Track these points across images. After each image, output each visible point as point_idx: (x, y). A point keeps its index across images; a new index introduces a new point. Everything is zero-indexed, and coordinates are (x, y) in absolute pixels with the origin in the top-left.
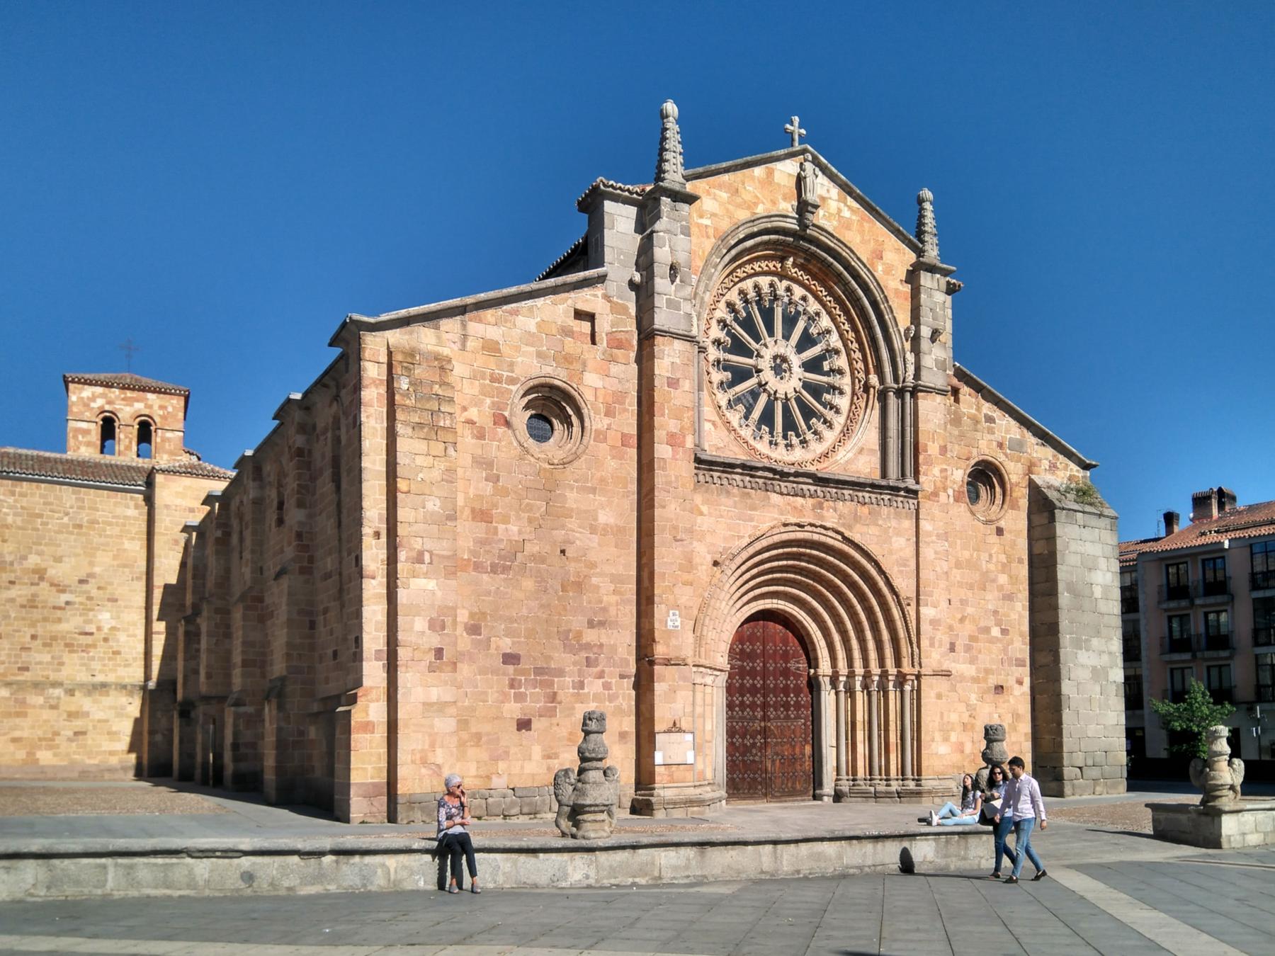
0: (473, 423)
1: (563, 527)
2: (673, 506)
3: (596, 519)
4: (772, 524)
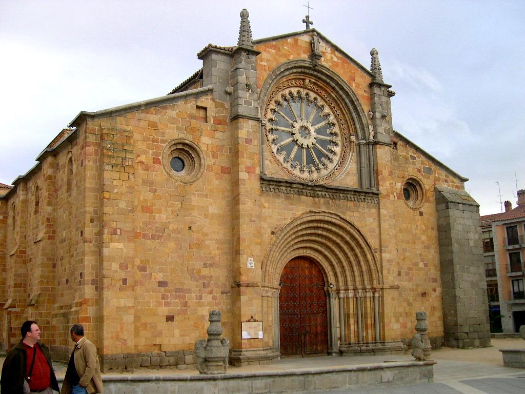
1: (190, 215)
2: (249, 203)
3: (207, 211)
4: (302, 212)
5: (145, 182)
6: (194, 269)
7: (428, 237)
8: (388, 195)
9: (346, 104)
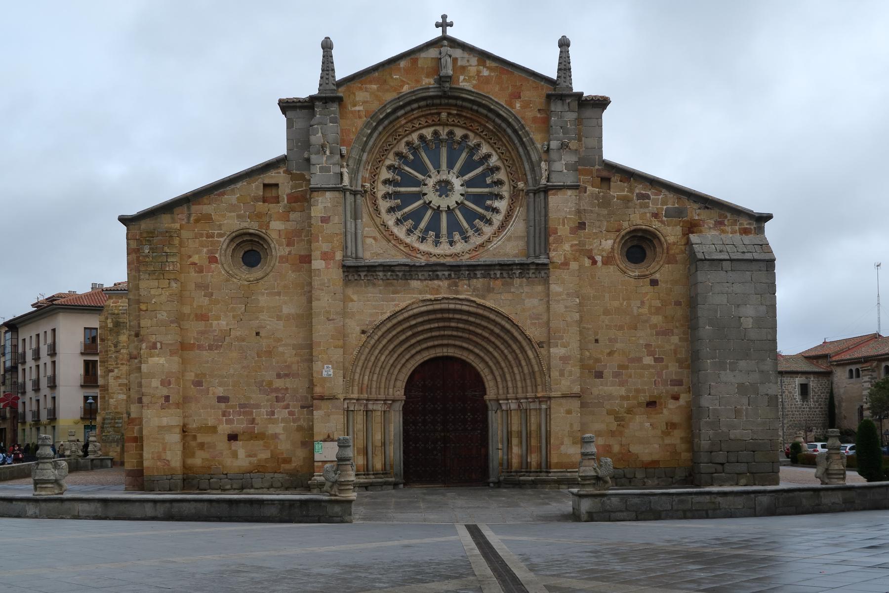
0: (196, 264)
1: (257, 318)
5: (198, 286)
6: (263, 381)
7: (666, 317)
8: (566, 264)
9: (509, 136)
